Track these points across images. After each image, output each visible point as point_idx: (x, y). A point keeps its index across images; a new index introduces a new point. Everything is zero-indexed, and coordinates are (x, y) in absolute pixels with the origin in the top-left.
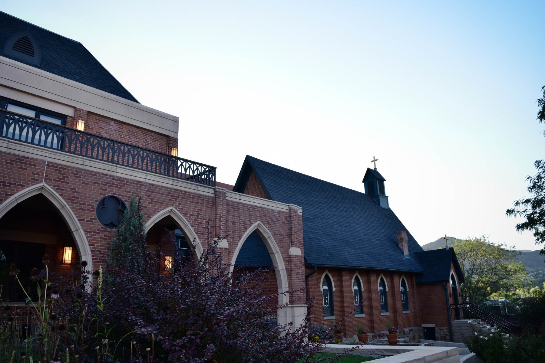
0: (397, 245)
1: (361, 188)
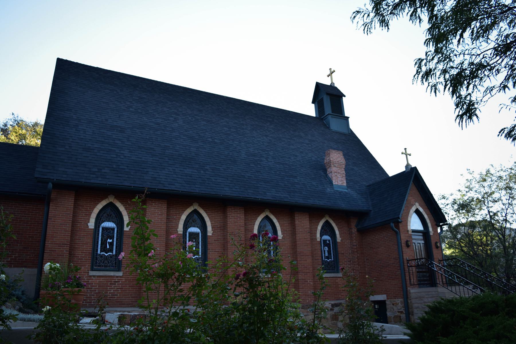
0: (325, 171)
1: (310, 111)
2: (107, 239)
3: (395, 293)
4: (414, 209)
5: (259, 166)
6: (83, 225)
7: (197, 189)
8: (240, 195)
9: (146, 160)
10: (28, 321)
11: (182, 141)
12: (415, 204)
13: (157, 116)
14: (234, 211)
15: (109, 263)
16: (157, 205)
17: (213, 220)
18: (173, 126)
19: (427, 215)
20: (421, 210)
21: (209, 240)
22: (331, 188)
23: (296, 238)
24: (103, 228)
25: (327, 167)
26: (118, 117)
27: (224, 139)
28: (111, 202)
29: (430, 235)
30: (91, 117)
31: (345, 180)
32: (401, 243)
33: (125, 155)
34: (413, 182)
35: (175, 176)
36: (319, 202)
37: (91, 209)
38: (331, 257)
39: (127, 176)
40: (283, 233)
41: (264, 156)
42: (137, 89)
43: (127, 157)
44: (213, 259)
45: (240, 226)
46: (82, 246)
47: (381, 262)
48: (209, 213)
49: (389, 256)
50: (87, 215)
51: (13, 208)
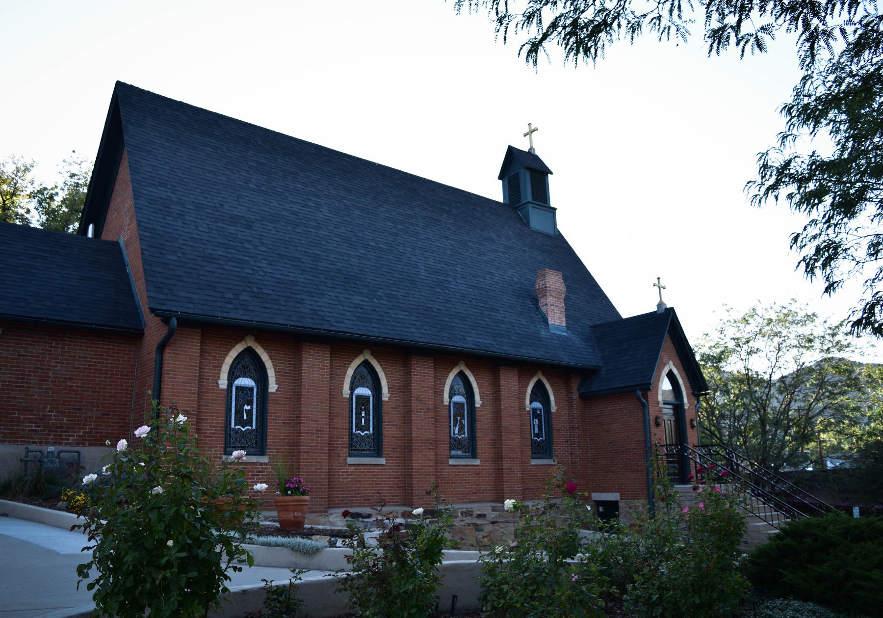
0: (536, 301)
1: (495, 191)
2: (244, 405)
3: (634, 491)
4: (666, 370)
5: (447, 292)
6: (211, 383)
7: (375, 330)
8: (433, 341)
9: (294, 279)
10: (274, 546)
11: (335, 246)
12: (668, 363)
13: (290, 199)
14: (420, 364)
15: (247, 443)
16: (317, 353)
17: (390, 377)
18: (317, 218)
19: (682, 378)
20: (675, 371)
21: (385, 408)
22: (546, 330)
23: (500, 406)
24: (237, 388)
25: (540, 296)
26: (236, 199)
27: (391, 242)
28: (250, 346)
29: (684, 410)
30: (197, 199)
31: (564, 317)
32: (649, 420)
33: (265, 270)
34: (668, 331)
35: (341, 307)
36: (535, 352)
37: (222, 357)
38: (542, 434)
39: (276, 307)
40: (482, 398)
41: (450, 273)
42: (249, 147)
43: (268, 274)
44: (389, 437)
45: (428, 387)
46: (209, 416)
47: (614, 445)
48: (385, 365)
49: (628, 437)
50: (216, 367)
51: (83, 348)
